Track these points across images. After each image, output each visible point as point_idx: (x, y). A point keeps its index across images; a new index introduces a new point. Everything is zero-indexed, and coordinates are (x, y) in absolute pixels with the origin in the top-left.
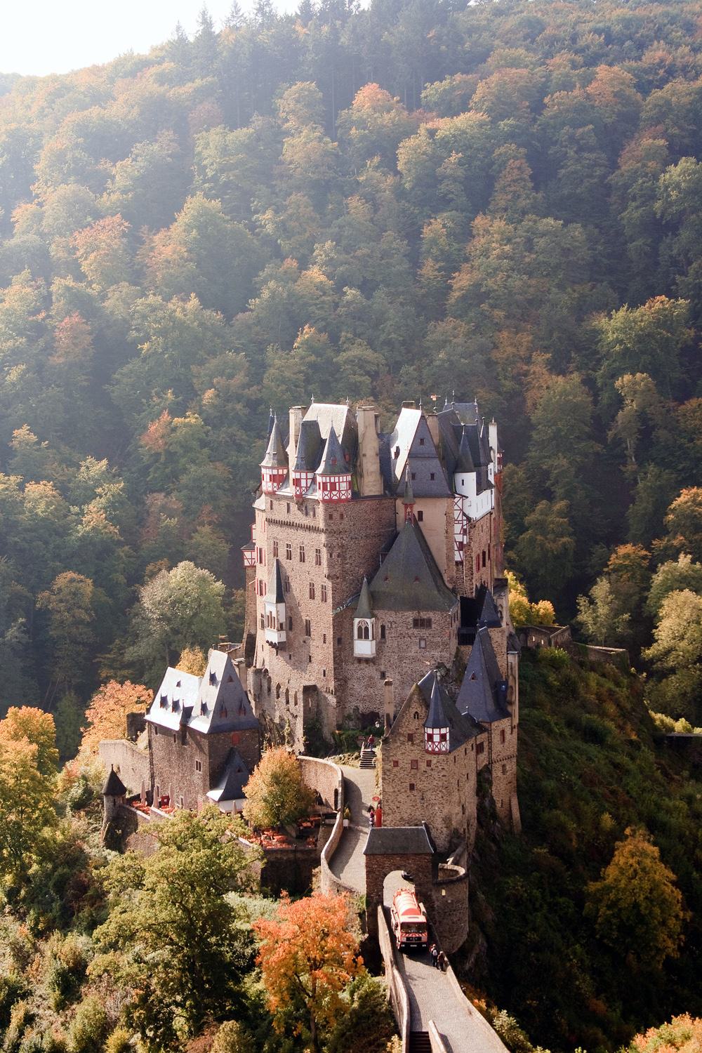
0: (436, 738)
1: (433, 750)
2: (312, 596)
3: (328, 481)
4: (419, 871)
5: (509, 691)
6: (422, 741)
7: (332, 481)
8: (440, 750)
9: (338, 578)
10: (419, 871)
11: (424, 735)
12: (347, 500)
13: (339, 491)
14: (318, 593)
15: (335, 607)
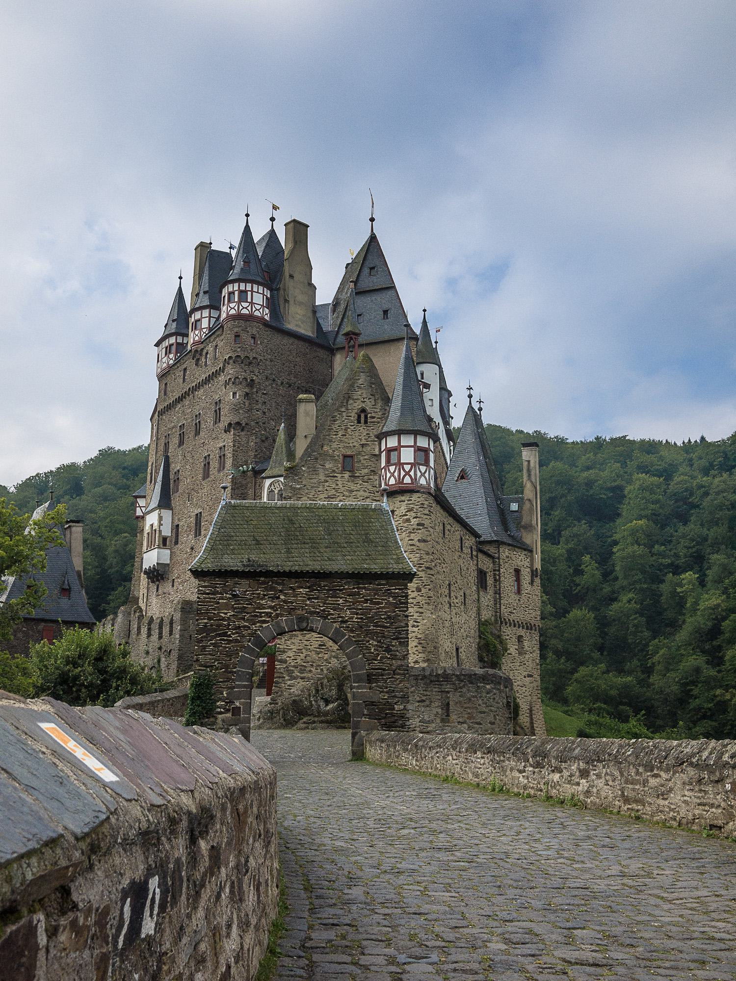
0: (408, 456)
1: (400, 481)
2: (206, 475)
3: (236, 288)
4: (368, 633)
5: (527, 505)
6: (374, 472)
7: (242, 287)
8: (414, 480)
9: (242, 430)
10: (368, 633)
11: (379, 456)
12: (266, 324)
13: (252, 303)
14: (214, 464)
15: (235, 465)
